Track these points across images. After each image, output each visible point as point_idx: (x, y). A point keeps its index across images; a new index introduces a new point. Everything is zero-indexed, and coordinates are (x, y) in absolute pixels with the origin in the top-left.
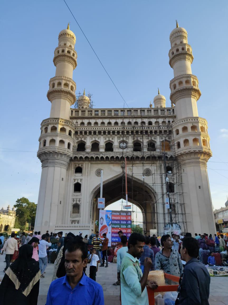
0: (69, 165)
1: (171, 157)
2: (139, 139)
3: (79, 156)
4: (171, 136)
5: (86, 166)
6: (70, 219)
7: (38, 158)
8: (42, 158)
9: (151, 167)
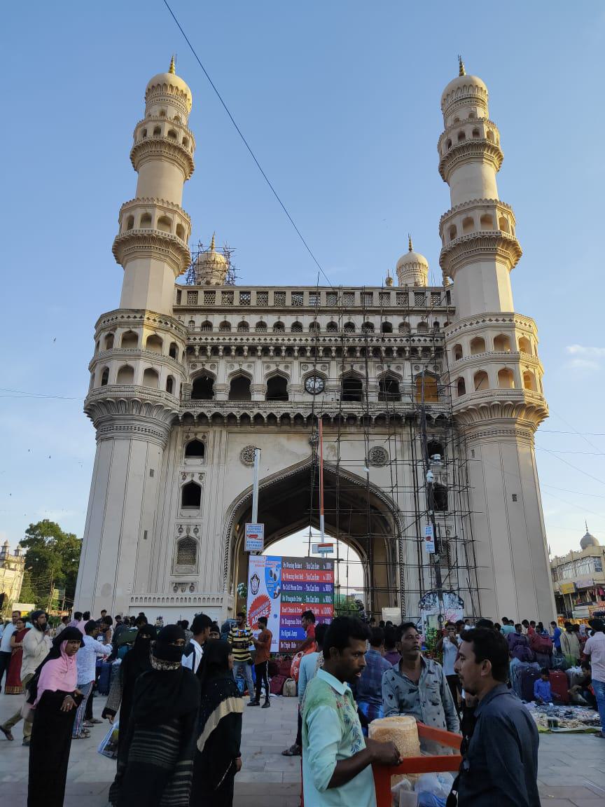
0: (170, 434)
1: (438, 417)
2: (357, 368)
3: (196, 411)
4: (440, 363)
5: (214, 438)
6: (170, 579)
7: (87, 415)
8: (98, 415)
9: (388, 442)
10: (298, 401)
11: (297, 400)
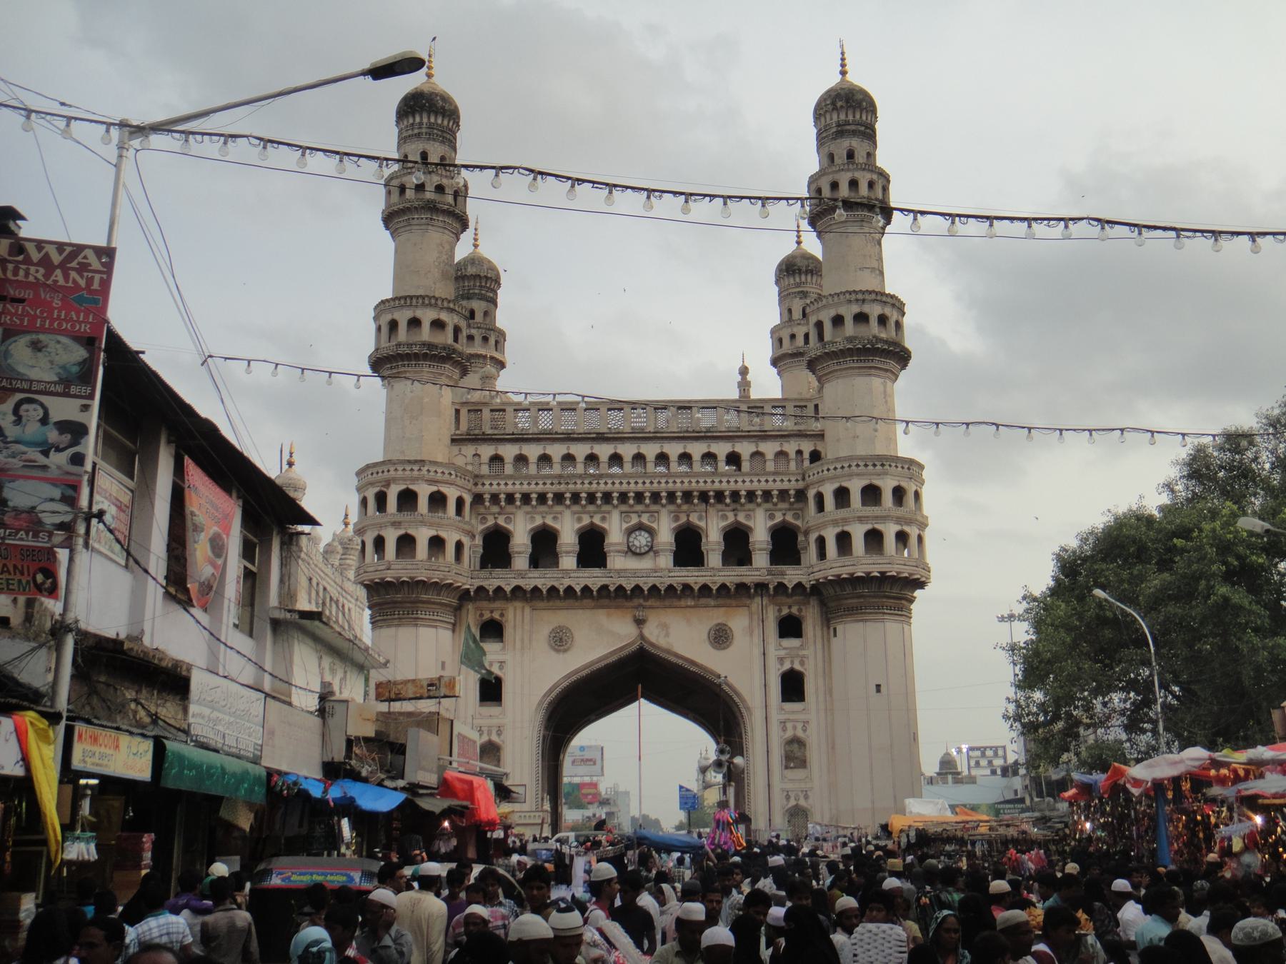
2: (694, 519)
5: (515, 617)
10: (622, 567)
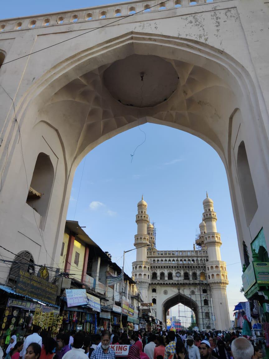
2: (187, 271)
3: (154, 282)
5: (158, 288)
11: (175, 279)
